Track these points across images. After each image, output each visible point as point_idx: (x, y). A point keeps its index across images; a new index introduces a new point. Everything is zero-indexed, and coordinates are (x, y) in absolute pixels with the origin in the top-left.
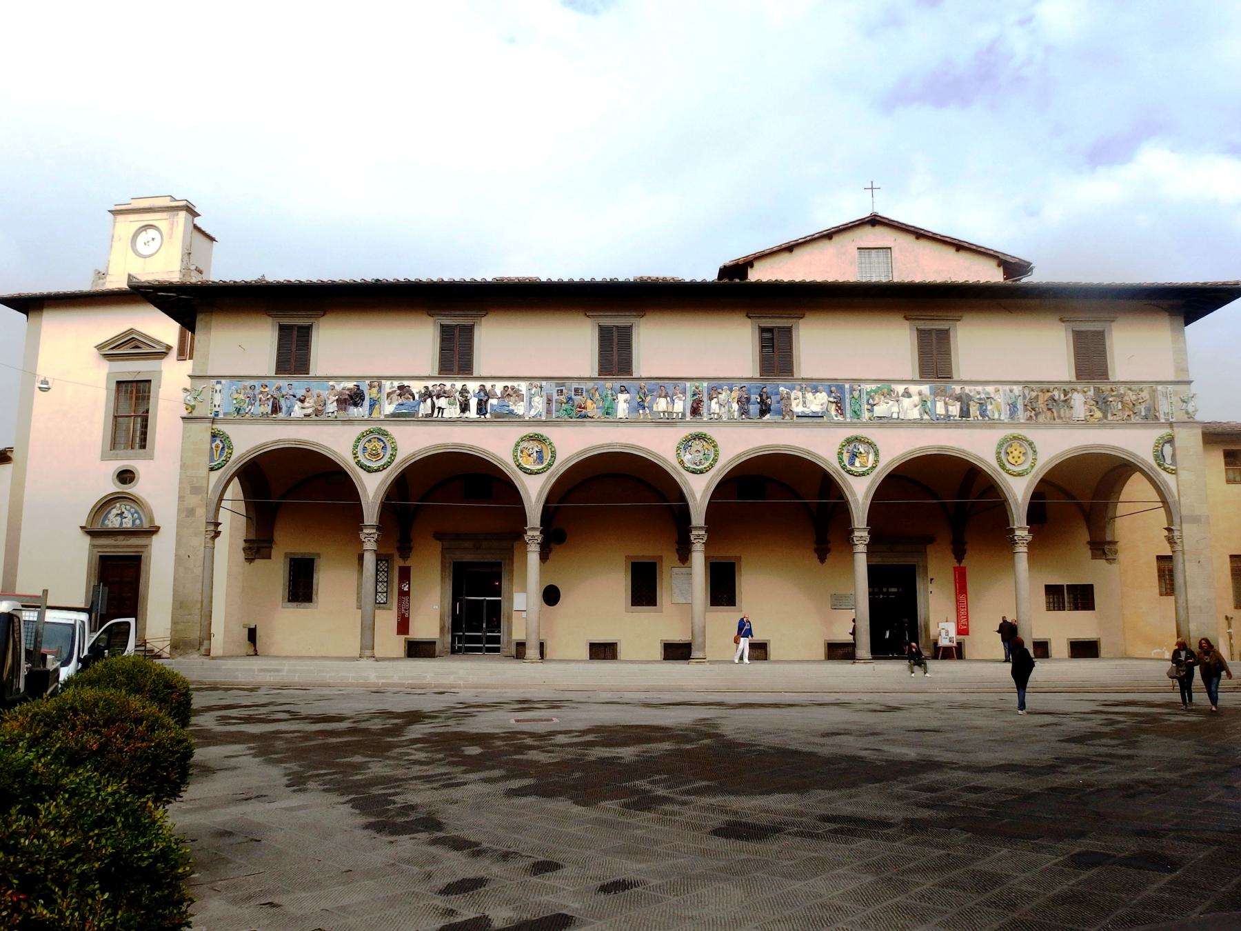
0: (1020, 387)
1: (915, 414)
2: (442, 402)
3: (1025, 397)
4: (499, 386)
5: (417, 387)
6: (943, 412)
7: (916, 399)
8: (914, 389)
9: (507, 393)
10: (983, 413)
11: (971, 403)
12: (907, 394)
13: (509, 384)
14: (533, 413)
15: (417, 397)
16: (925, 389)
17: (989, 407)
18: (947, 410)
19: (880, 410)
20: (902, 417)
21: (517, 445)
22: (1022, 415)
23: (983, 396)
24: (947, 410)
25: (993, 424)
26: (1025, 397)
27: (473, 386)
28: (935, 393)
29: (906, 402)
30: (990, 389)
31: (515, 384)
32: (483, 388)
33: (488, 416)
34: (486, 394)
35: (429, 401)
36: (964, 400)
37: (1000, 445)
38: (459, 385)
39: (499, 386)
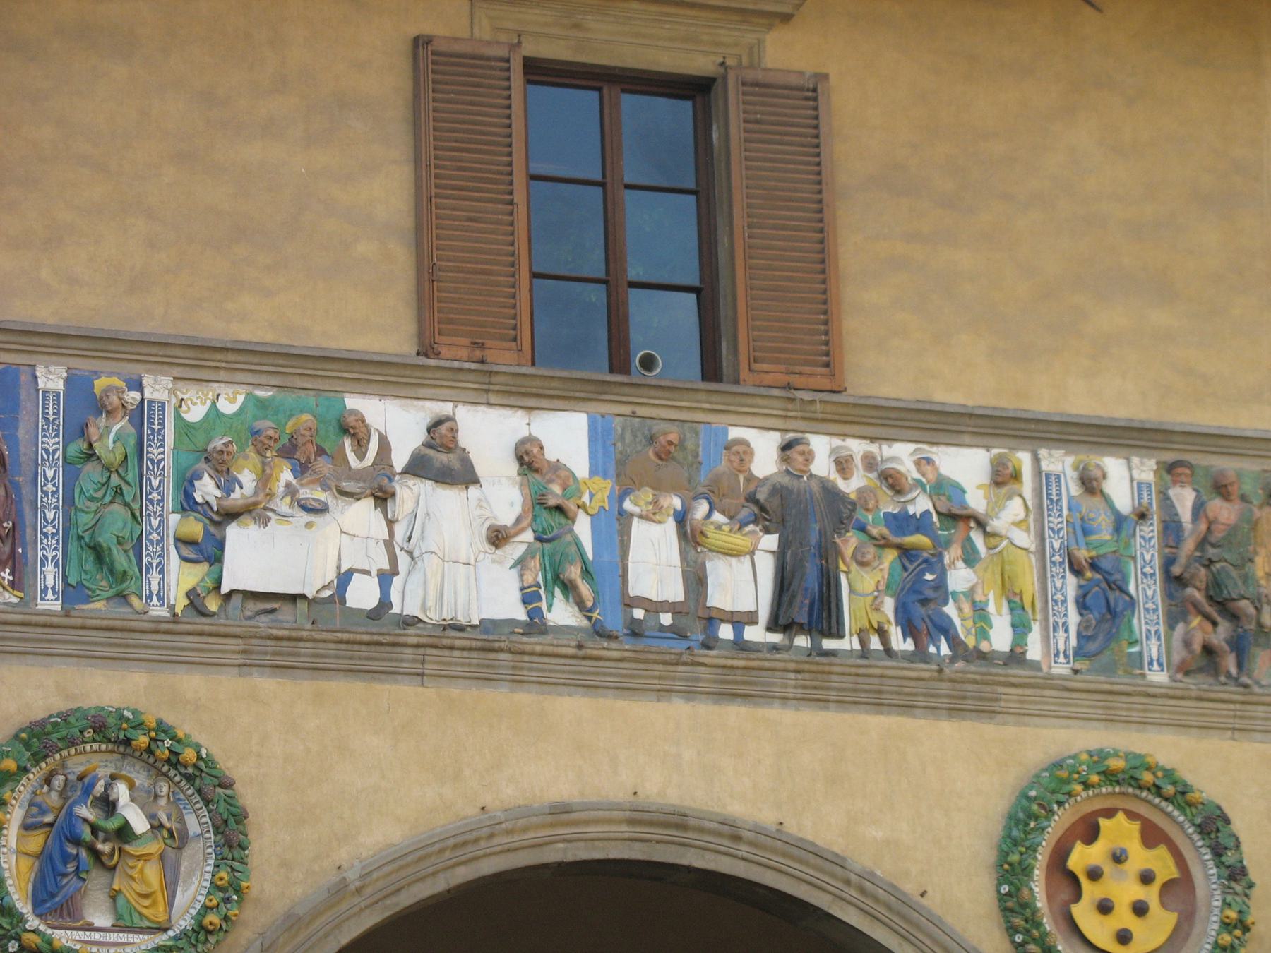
0: (1146, 470)
1: (495, 594)
3: (1171, 528)
6: (675, 591)
7: (503, 497)
8: (489, 432)
10: (920, 607)
11: (850, 542)
12: (444, 463)
16: (567, 436)
17: (959, 577)
18: (696, 581)
19: (260, 558)
20: (406, 601)
22: (1152, 636)
23: (921, 504)
24: (696, 581)
25: (980, 685)
26: (1171, 528)
28: (637, 465)
29: (446, 517)
30: (965, 466)
36: (807, 528)
37: (1023, 821)
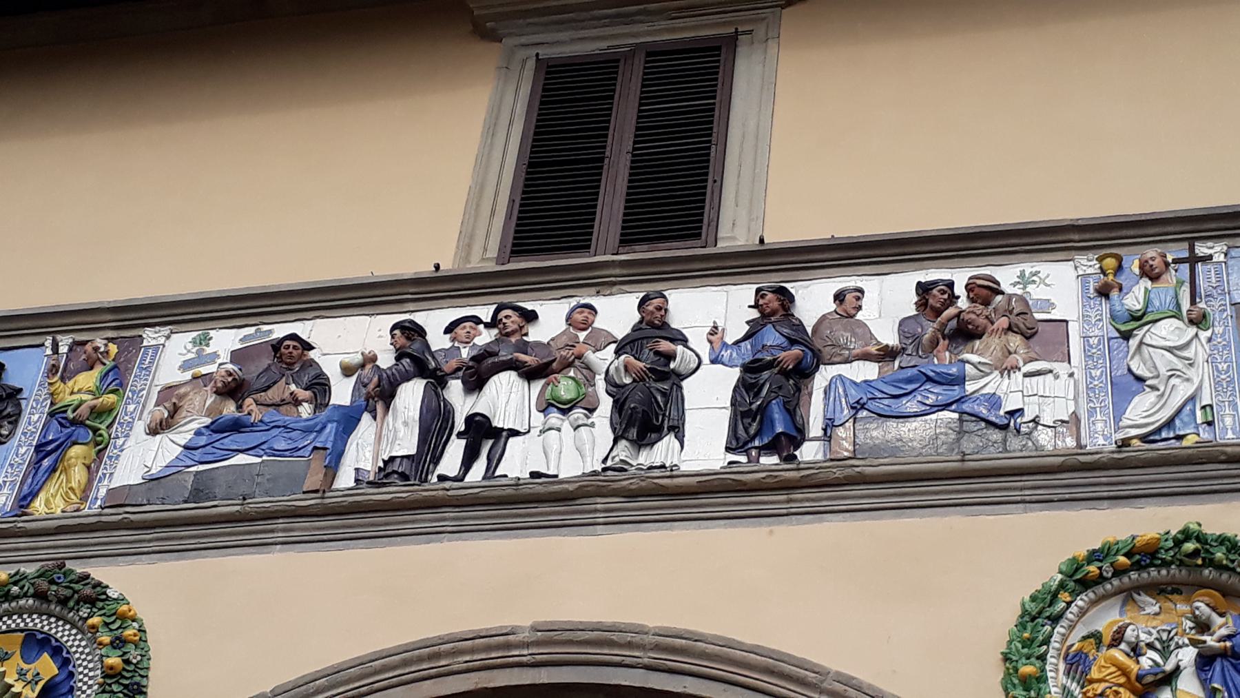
2: (506, 398)
4: (888, 301)
5: (345, 343)
9: (950, 325)
13: (960, 276)
14: (1143, 411)
15: (342, 393)
21: (1041, 613)
27: (711, 312)
31: (1007, 275)
32: (776, 309)
33: (809, 452)
34: (797, 334)
35: (411, 395)
38: (618, 312)
39: (888, 301)
